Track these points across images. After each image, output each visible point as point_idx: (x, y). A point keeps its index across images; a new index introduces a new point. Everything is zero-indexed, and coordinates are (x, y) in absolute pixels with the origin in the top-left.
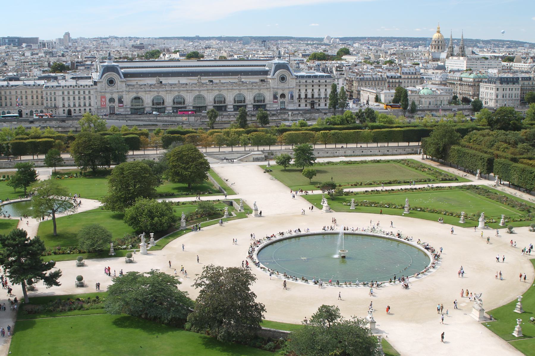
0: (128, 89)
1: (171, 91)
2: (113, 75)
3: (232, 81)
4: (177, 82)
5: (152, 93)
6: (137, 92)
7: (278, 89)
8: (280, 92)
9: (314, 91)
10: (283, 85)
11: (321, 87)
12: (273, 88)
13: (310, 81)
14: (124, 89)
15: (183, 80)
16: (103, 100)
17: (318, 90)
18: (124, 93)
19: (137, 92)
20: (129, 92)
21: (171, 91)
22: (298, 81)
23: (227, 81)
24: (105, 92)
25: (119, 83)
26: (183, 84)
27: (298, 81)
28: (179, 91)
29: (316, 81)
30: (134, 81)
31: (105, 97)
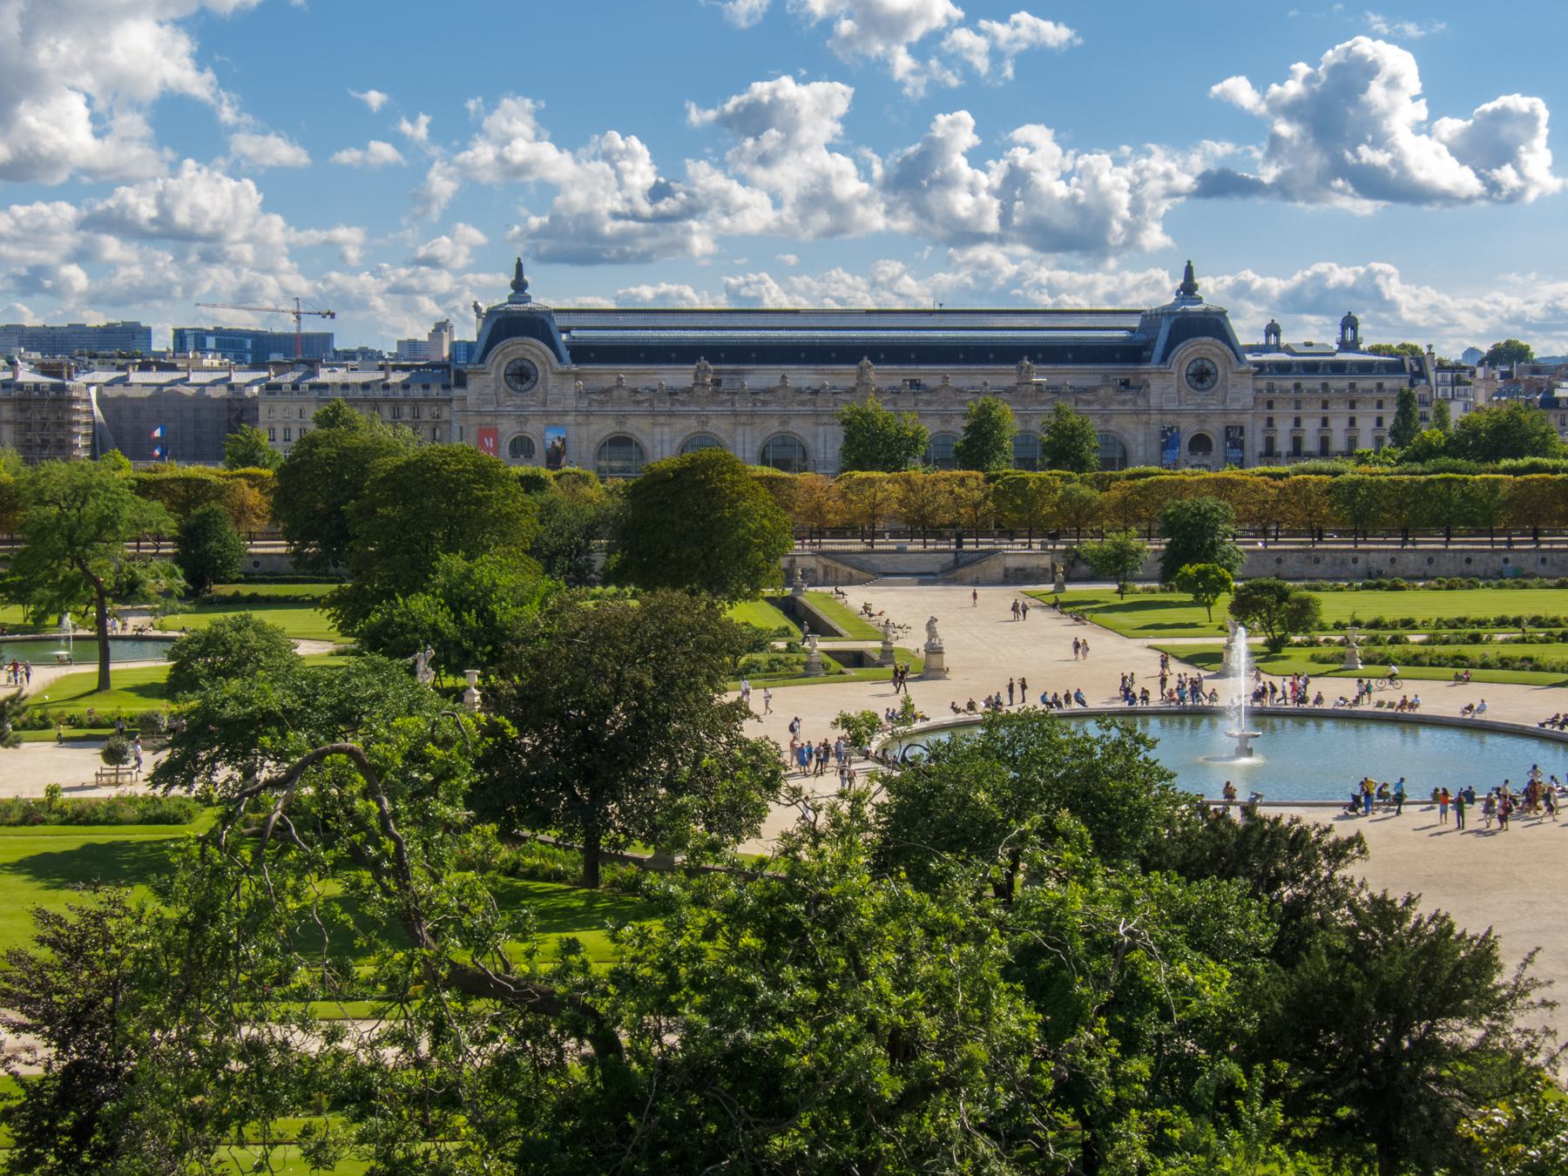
0: (584, 405)
1: (752, 414)
2: (531, 349)
3: (993, 382)
4: (775, 382)
5: (680, 424)
6: (621, 418)
7: (1178, 413)
8: (1189, 428)
9: (1332, 424)
10: (1200, 398)
11: (1360, 408)
12: (1161, 411)
13: (1311, 383)
14: (571, 403)
15: (803, 376)
16: (489, 443)
17: (1344, 423)
18: (569, 419)
19: (621, 418)
20: (588, 414)
21: (752, 414)
22: (1262, 384)
23: (977, 381)
24: (496, 414)
25: (552, 381)
26: (799, 391)
27: (1262, 384)
28: (785, 418)
29: (1339, 383)
30: (605, 375)
31: (493, 432)
